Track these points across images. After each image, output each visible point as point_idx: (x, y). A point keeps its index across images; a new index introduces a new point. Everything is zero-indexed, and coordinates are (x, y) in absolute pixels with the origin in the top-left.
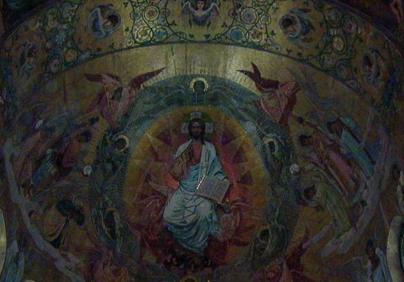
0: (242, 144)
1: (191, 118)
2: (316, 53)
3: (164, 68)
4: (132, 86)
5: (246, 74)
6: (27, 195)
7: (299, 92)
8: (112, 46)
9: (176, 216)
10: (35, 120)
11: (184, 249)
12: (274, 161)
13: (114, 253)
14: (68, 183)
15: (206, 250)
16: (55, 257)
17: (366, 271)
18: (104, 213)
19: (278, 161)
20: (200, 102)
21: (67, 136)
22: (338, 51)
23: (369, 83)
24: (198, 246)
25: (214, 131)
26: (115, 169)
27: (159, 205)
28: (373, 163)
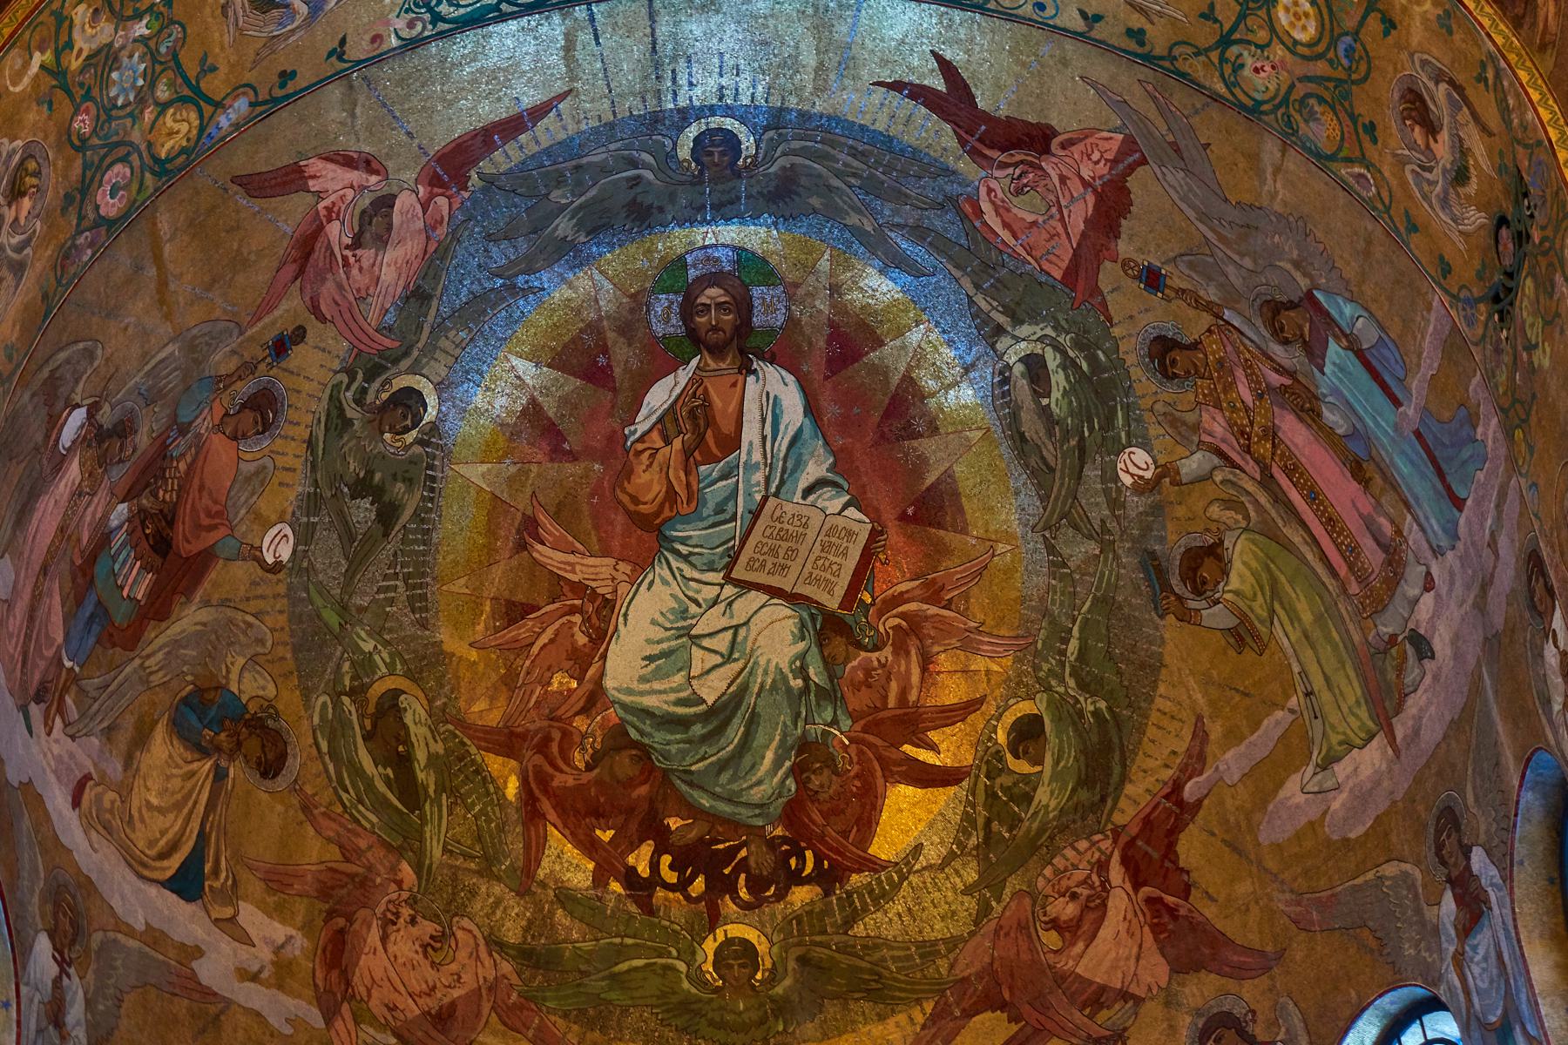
0: (909, 369)
1: (692, 274)
2: (1205, 35)
3: (562, 97)
4: (435, 182)
5: (912, 96)
6: (58, 720)
7: (1140, 170)
8: (338, 53)
9: (658, 675)
10: (54, 423)
11: (694, 811)
12: (1050, 434)
13: (418, 868)
14: (205, 615)
15: (793, 813)
16: (189, 942)
17: (1436, 931)
18: (361, 705)
19: (1066, 435)
20: (725, 210)
21: (183, 430)
22: (1296, 42)
23: (1425, 197)
24: (757, 794)
25: (791, 321)
26: (387, 515)
27: (582, 640)
28: (1459, 503)
